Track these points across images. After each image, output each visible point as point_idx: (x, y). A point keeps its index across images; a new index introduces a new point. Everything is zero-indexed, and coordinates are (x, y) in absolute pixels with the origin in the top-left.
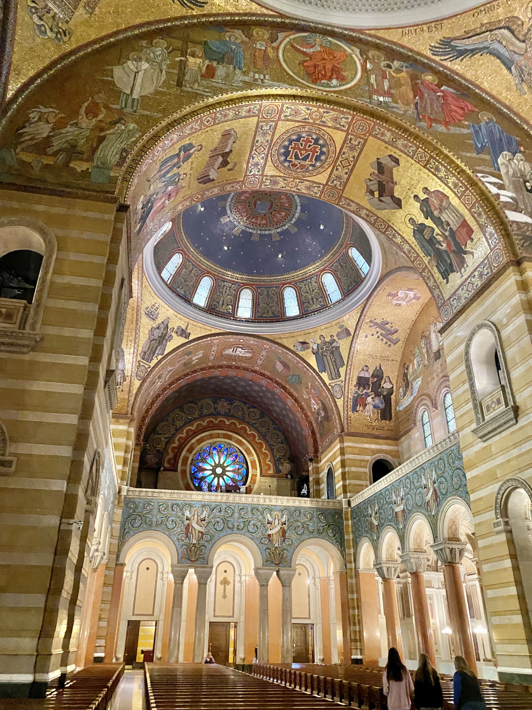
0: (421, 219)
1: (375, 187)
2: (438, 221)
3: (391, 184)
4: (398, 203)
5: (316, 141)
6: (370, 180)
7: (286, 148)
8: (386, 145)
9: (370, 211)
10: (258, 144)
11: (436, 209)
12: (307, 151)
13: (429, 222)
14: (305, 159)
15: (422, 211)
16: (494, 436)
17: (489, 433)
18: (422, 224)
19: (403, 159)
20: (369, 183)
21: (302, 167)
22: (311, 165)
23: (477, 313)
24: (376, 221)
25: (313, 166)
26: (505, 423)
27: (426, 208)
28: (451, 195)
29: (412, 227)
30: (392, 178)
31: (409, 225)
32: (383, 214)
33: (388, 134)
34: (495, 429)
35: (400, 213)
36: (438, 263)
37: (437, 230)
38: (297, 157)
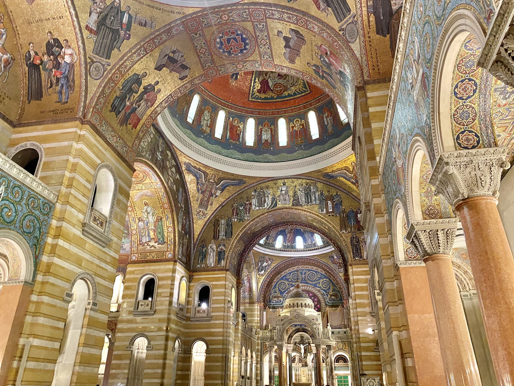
0: (145, 82)
1: (176, 56)
2: (141, 98)
3: (172, 68)
4: (159, 68)
5: (229, 52)
6: (182, 56)
7: (246, 44)
8: (193, 78)
9: (163, 43)
10: (267, 46)
11: (148, 96)
12: (231, 45)
13: (141, 89)
14: (229, 40)
15: (149, 85)
16: (92, 240)
17: (92, 235)
18: (141, 83)
19: (181, 83)
20: (181, 54)
21: (227, 34)
22: (222, 37)
23: (121, 168)
24: (154, 43)
25: (220, 38)
26: (102, 242)
27: (150, 89)
28: (153, 108)
29: (141, 74)
30: (174, 71)
31: (142, 72)
32: (156, 53)
33: (197, 82)
34: (95, 237)
35: (153, 66)
36: (119, 98)
37: (136, 95)
38: (235, 39)
